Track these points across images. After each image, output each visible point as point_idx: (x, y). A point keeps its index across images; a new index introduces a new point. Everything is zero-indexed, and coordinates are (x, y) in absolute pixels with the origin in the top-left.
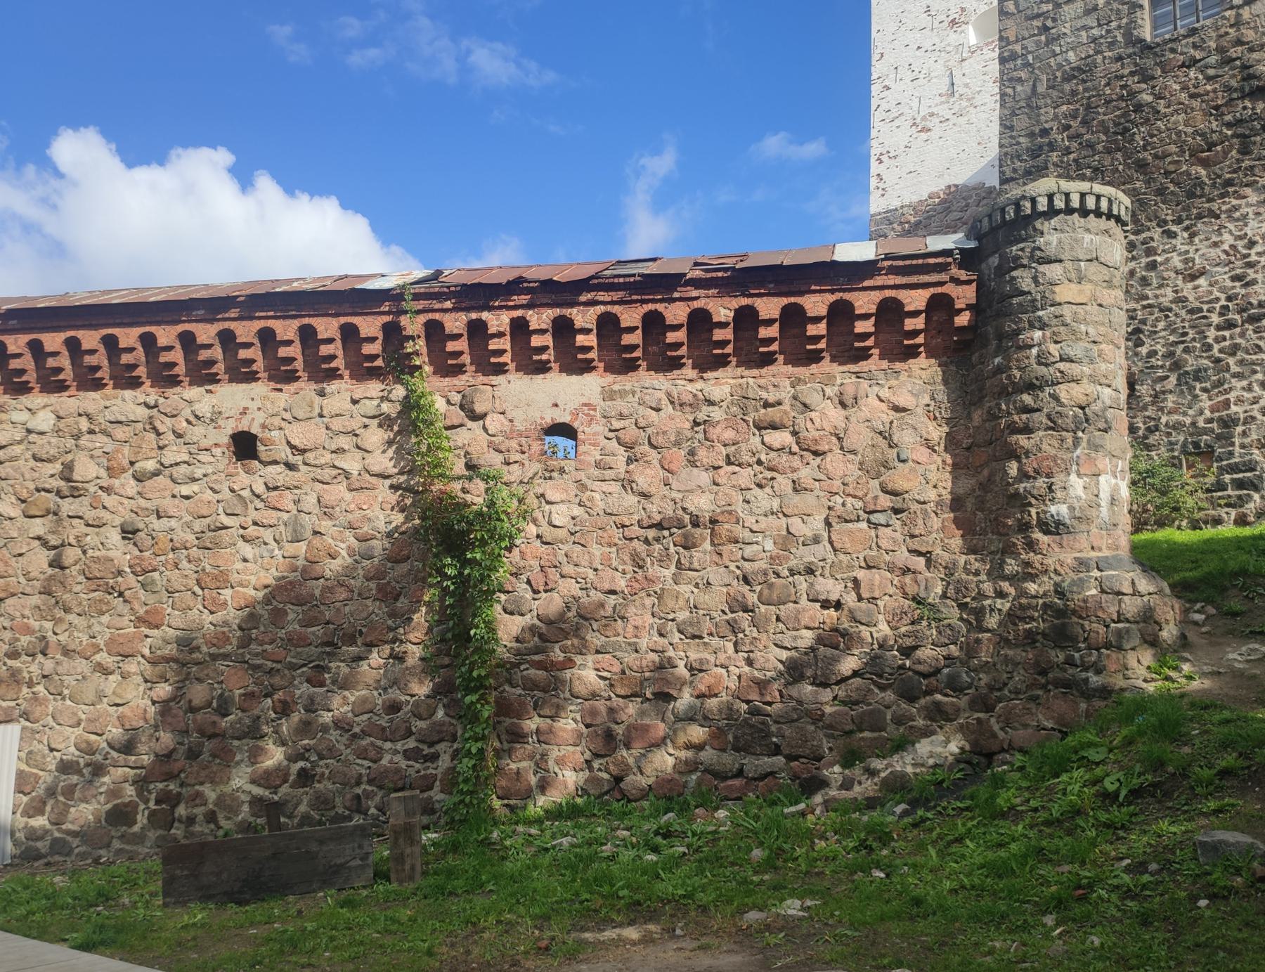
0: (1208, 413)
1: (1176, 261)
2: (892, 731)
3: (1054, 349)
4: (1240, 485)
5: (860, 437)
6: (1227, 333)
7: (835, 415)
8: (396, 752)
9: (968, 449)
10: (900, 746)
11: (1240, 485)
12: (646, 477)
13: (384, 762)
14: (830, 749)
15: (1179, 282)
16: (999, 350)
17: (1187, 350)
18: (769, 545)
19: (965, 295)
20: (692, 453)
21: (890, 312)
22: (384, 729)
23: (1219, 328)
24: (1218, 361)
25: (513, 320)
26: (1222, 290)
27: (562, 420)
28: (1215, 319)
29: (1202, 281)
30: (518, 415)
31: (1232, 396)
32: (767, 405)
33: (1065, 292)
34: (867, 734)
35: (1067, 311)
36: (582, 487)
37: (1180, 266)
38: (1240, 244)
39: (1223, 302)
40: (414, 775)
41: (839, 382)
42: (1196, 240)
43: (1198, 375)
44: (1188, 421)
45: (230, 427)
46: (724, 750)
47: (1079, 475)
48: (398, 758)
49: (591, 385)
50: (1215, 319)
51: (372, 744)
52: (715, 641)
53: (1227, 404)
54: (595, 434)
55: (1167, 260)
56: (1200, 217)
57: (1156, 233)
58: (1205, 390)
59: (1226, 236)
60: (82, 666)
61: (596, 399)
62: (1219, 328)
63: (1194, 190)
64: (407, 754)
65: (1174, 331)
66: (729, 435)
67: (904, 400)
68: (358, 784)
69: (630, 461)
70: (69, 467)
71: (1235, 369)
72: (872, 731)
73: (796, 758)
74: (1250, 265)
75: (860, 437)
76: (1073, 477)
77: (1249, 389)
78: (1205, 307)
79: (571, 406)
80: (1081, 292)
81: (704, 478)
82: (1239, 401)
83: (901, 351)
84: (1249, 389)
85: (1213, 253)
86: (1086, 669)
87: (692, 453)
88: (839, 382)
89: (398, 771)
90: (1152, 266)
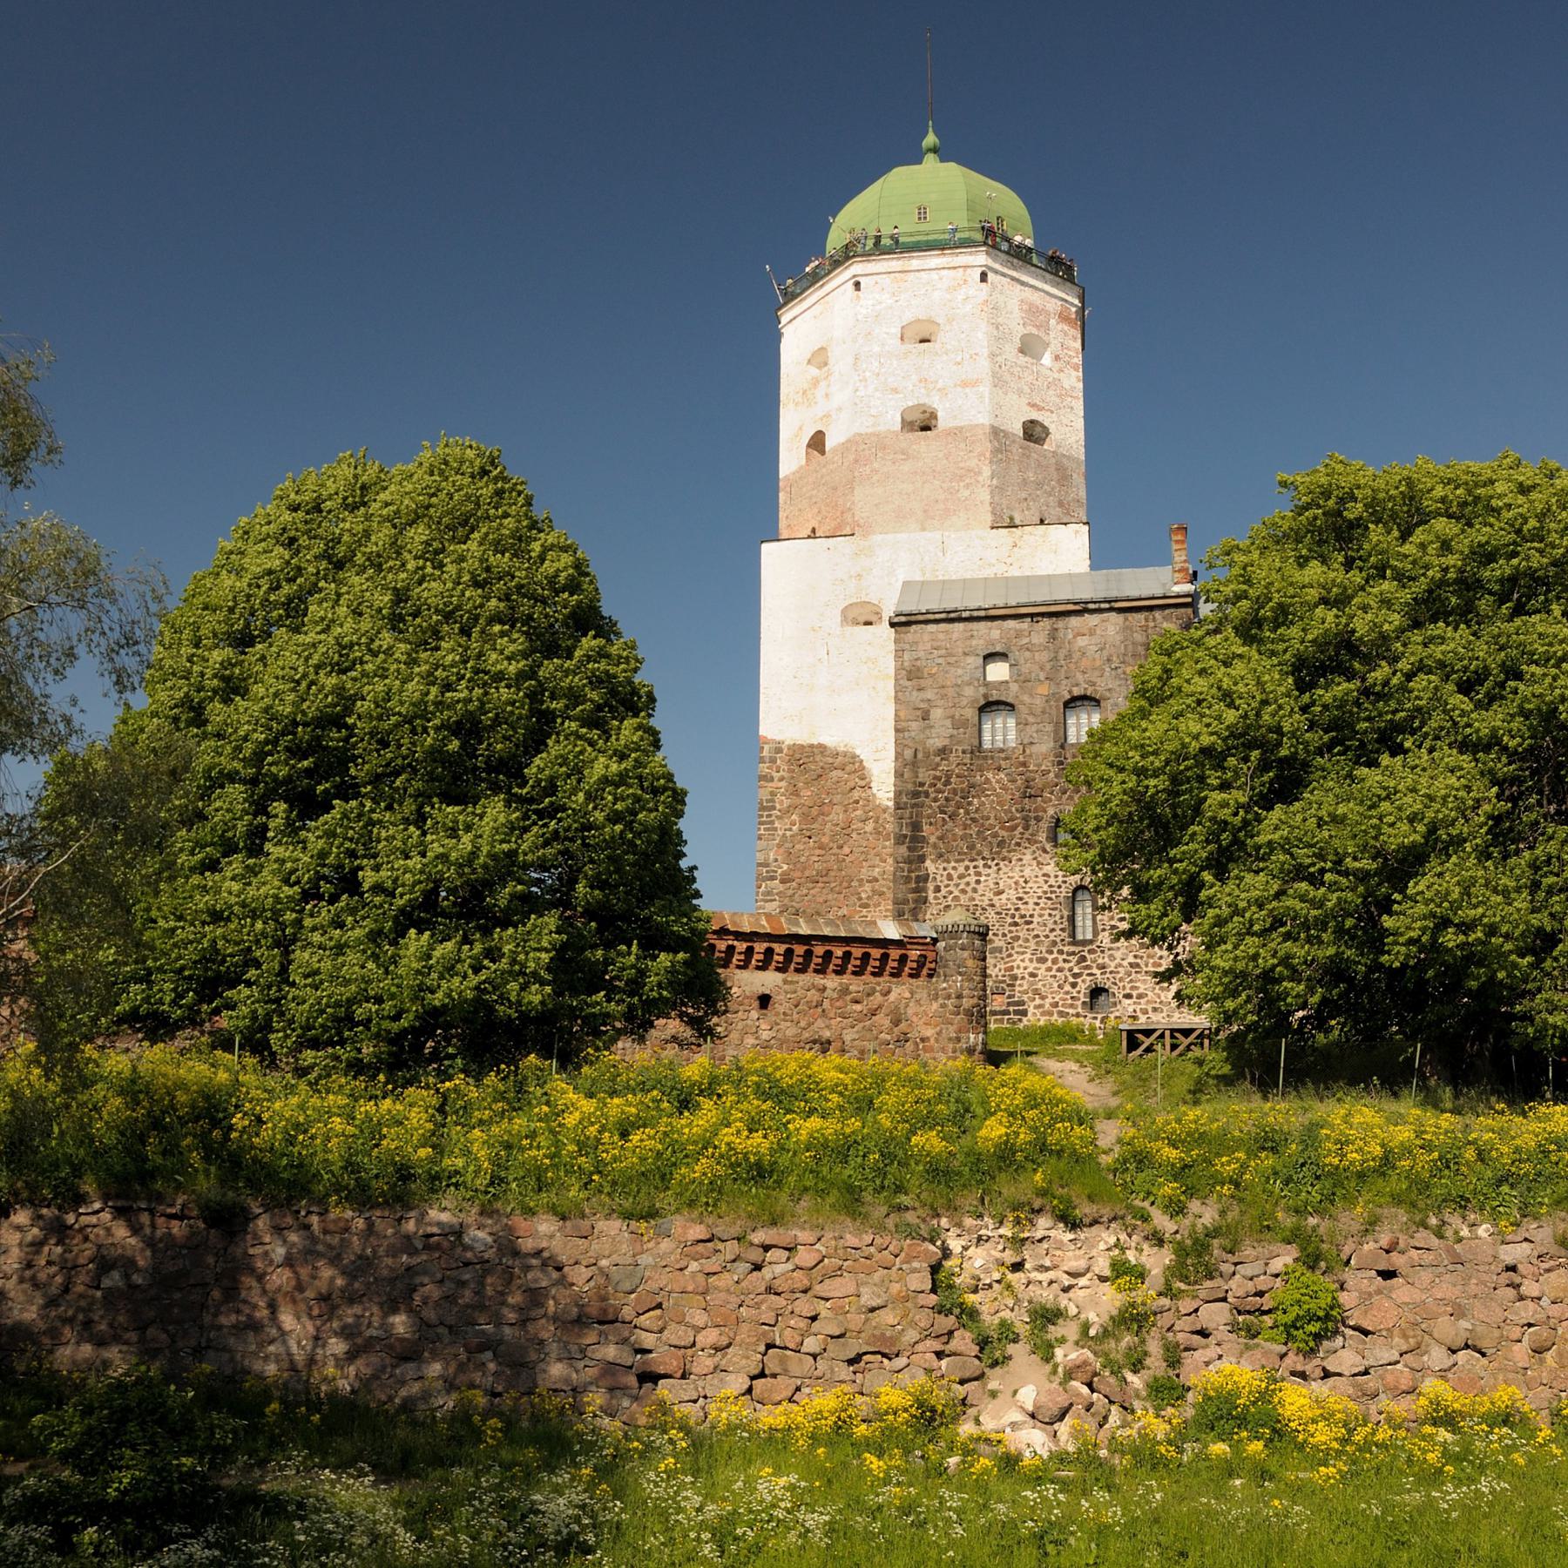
4: (1016, 1012)
11: (1016, 1012)
28: (1009, 920)
53: (1012, 968)
57: (981, 863)
90: (978, 882)
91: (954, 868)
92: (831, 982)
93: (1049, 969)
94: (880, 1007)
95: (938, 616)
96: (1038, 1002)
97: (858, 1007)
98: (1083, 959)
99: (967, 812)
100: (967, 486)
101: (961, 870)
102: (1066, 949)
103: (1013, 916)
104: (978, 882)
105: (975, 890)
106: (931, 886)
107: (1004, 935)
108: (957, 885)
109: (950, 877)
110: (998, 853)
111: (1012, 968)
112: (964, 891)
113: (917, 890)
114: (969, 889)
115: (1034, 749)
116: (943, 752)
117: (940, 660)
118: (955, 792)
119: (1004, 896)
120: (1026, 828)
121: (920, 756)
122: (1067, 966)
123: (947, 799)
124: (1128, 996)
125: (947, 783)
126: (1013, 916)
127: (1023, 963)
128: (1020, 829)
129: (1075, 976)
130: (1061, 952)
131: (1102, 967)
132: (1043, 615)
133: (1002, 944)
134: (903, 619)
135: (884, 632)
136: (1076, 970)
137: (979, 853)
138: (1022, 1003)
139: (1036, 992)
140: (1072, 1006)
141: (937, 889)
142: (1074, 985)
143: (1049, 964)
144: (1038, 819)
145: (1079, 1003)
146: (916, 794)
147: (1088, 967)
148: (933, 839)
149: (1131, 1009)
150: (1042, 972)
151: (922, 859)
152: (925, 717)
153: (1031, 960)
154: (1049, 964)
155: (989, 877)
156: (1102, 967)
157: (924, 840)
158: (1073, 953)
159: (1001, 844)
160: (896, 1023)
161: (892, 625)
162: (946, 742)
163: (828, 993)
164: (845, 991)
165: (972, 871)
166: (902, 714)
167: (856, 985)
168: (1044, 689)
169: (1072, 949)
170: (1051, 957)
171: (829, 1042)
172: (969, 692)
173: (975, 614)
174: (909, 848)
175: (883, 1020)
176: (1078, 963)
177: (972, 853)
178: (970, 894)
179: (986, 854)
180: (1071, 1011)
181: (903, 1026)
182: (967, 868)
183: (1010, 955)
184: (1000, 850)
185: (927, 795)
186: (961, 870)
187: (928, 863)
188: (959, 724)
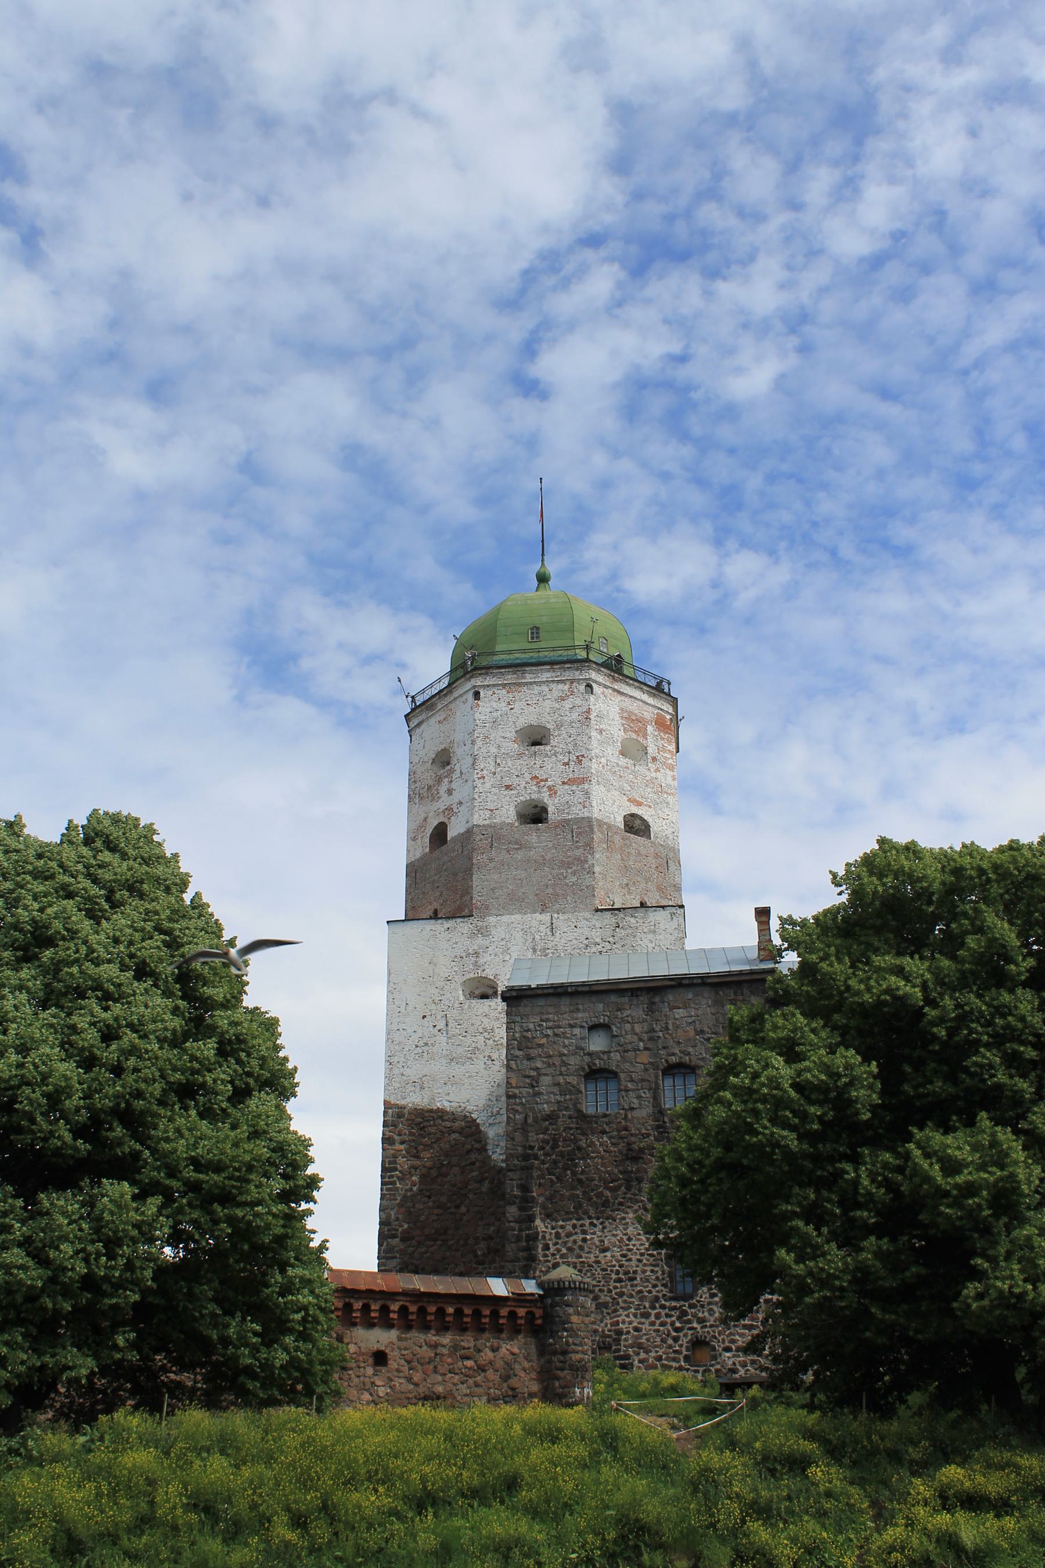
1: (596, 1241)
3: (570, 1340)
5: (499, 1364)
6: (618, 1285)
7: (490, 1354)
12: (417, 1377)
16: (552, 1337)
17: (600, 1290)
19: (538, 1313)
20: (435, 1367)
21: (513, 1315)
23: (615, 1281)
24: (614, 1299)
26: (618, 1261)
28: (614, 1276)
29: (608, 1254)
31: (620, 1319)
32: (464, 1348)
33: (574, 1319)
35: (574, 1326)
36: (391, 1380)
37: (598, 1243)
38: (625, 1238)
43: (605, 1305)
49: (393, 1334)
50: (614, 1276)
53: (617, 1323)
55: (592, 1239)
56: (607, 1218)
57: (587, 1222)
58: (608, 1314)
59: (619, 1232)
62: (615, 1281)
63: (606, 1204)
65: (594, 1279)
66: (449, 1360)
67: (516, 1350)
69: (410, 1369)
71: (622, 1304)
74: (630, 1250)
75: (499, 1364)
77: (628, 1316)
81: (440, 1378)
82: (624, 1322)
83: (516, 1331)
84: (628, 1316)
85: (613, 1239)
87: (435, 1367)
90: (584, 1240)
92: (446, 1339)
93: (653, 1324)
95: (546, 991)
96: (643, 1355)
97: (469, 1363)
98: (684, 1313)
99: (574, 1173)
100: (574, 873)
101: (569, 1228)
102: (667, 1304)
105: (581, 1248)
108: (565, 1243)
111: (617, 1323)
115: (636, 1114)
116: (552, 1117)
117: (549, 1032)
118: (562, 1154)
120: (629, 1188)
121: (530, 1121)
122: (669, 1320)
123: (555, 1162)
124: (728, 1349)
126: (618, 1273)
127: (627, 1320)
129: (677, 1330)
130: (663, 1307)
131: (701, 1321)
132: (641, 989)
134: (514, 994)
135: (498, 1005)
136: (678, 1325)
137: (586, 1213)
138: (627, 1357)
139: (640, 1346)
140: (674, 1360)
141: (546, 1247)
142: (676, 1339)
143: (653, 1318)
144: (640, 1180)
145: (681, 1357)
146: (526, 1157)
147: (689, 1322)
148: (541, 1200)
149: (730, 1362)
150: (646, 1327)
151: (531, 1219)
152: (534, 1082)
153: (635, 1316)
154: (653, 1318)
155: (594, 1236)
156: (701, 1321)
158: (675, 1308)
159: (606, 1204)
160: (506, 1378)
161: (504, 999)
166: (513, 1082)
167: (468, 1341)
168: (645, 1057)
169: (674, 1304)
170: (653, 1312)
172: (573, 1061)
173: (580, 989)
176: (679, 1318)
177: (579, 1212)
179: (592, 1213)
180: (674, 1364)
183: (615, 1311)
184: (605, 1211)
185: (536, 1157)
186: (569, 1228)
187: (538, 1222)
188: (565, 1090)
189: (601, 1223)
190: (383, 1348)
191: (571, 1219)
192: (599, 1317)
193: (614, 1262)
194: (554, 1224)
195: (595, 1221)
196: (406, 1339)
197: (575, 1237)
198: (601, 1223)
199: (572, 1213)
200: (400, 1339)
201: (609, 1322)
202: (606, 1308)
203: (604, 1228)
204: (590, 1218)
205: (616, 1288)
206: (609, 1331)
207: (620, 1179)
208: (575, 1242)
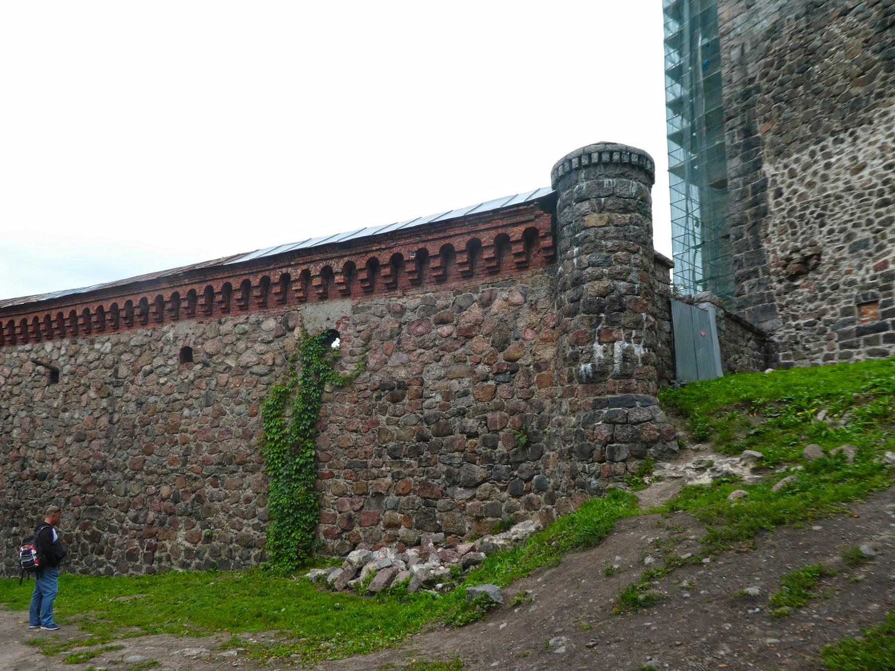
0: (872, 272)
2: (506, 517)
6: (883, 210)
8: (249, 526)
9: (553, 328)
10: (506, 527)
13: (243, 531)
14: (470, 529)
15: (848, 176)
17: (855, 226)
18: (439, 398)
22: (243, 512)
23: (878, 206)
25: (303, 271)
27: (332, 328)
28: (875, 200)
30: (309, 327)
34: (489, 519)
39: (879, 187)
40: (257, 539)
41: (481, 290)
42: (858, 142)
43: (864, 244)
44: (859, 279)
45: (180, 344)
46: (410, 528)
47: (600, 343)
48: (250, 529)
51: (238, 521)
52: (407, 460)
54: (349, 335)
55: (839, 160)
60: (119, 476)
61: (348, 313)
62: (878, 206)
63: (856, 105)
64: (255, 527)
68: (231, 543)
70: (117, 371)
72: (492, 517)
73: (450, 534)
76: (596, 345)
78: (867, 192)
79: (337, 319)
80: (601, 218)
86: (591, 476)
88: (481, 290)
89: (249, 536)
91: (797, 161)
92: (413, 300)
94: (478, 324)
97: (446, 329)
101: (806, 158)
103: (881, 193)
104: (828, 166)
105: (825, 178)
106: (771, 193)
107: (869, 222)
108: (802, 180)
109: (792, 174)
110: (852, 119)
112: (811, 185)
113: (755, 203)
114: (817, 179)
119: (865, 173)
121: (748, 49)
123: (782, 84)
125: (782, 62)
128: (882, 74)
133: (868, 234)
141: (779, 193)
148: (769, 138)
151: (758, 165)
157: (759, 142)
159: (856, 105)
162: (776, 17)
163: (409, 316)
164: (429, 307)
165: (819, 156)
167: (444, 298)
171: (403, 386)
174: (744, 159)
175: (481, 344)
178: (819, 184)
179: (836, 125)
181: (512, 350)
182: (813, 154)
183: (881, 248)
185: (758, 89)
186: (806, 158)
189: (852, 134)
190: (334, 327)
191: (807, 146)
192: (856, 262)
193: (875, 181)
194: (785, 161)
195: (842, 136)
196: (363, 309)
197: (814, 168)
198: (852, 134)
199: (809, 137)
200: (355, 310)
201: (871, 265)
202: (866, 247)
203: (855, 139)
204: (833, 134)
205: (878, 215)
206: (874, 278)
207: (876, 62)
208: (815, 173)
